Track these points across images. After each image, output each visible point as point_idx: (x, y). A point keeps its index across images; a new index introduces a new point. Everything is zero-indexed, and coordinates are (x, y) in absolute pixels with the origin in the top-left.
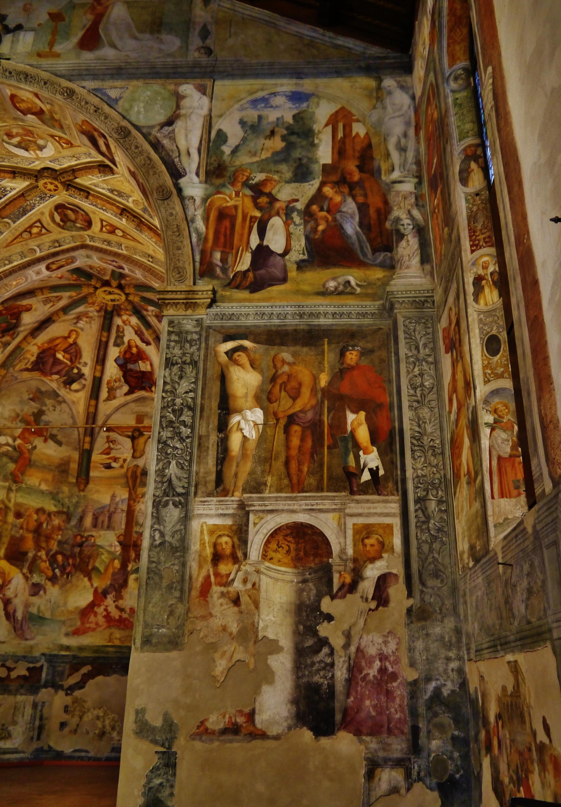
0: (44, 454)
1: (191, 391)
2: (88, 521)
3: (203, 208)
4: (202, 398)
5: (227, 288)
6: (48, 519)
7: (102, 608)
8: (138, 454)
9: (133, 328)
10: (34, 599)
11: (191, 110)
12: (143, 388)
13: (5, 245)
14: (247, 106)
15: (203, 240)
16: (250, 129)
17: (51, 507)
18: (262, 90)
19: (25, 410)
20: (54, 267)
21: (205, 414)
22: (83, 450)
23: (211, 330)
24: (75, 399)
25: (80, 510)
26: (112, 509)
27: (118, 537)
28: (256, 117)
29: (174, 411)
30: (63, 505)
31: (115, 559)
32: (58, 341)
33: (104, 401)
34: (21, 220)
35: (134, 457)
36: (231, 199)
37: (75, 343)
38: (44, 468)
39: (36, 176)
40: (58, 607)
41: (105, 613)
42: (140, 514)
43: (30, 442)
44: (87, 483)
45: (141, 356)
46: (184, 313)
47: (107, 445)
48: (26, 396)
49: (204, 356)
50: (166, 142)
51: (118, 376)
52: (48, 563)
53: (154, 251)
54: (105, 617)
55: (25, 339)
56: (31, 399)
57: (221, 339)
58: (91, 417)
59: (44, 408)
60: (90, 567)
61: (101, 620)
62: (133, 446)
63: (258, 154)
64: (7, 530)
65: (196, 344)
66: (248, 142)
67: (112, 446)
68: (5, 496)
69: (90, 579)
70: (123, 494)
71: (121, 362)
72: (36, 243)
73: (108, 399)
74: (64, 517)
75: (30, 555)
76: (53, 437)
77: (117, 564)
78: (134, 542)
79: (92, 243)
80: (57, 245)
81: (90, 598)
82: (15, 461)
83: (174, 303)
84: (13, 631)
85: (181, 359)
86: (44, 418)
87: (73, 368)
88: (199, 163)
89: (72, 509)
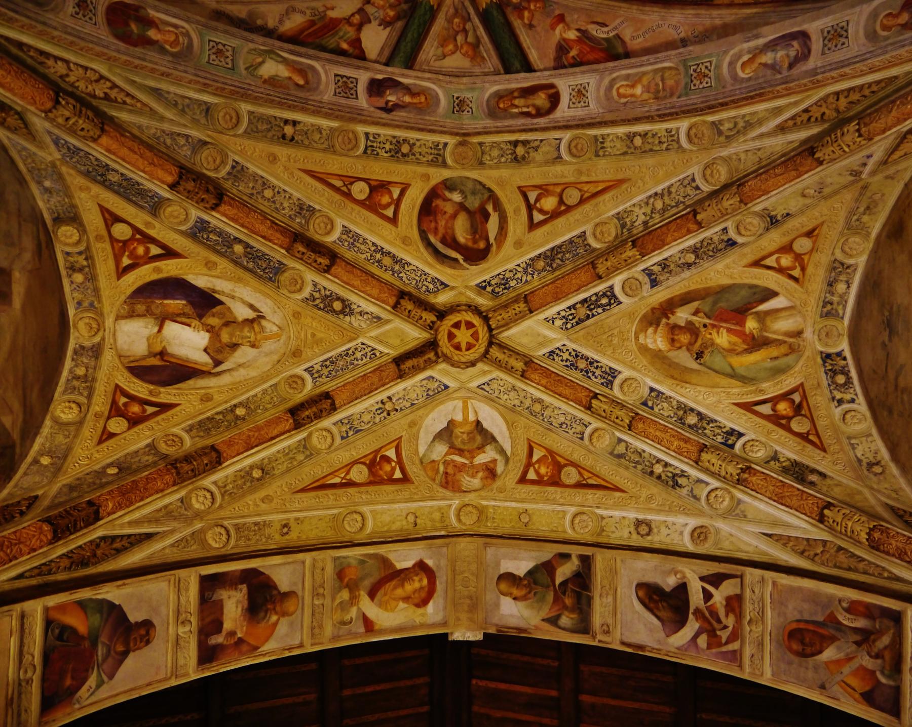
13: (624, 186)
20: (541, 99)
34: (567, 237)
53: (273, 159)
72: (558, 168)
80: (520, 151)
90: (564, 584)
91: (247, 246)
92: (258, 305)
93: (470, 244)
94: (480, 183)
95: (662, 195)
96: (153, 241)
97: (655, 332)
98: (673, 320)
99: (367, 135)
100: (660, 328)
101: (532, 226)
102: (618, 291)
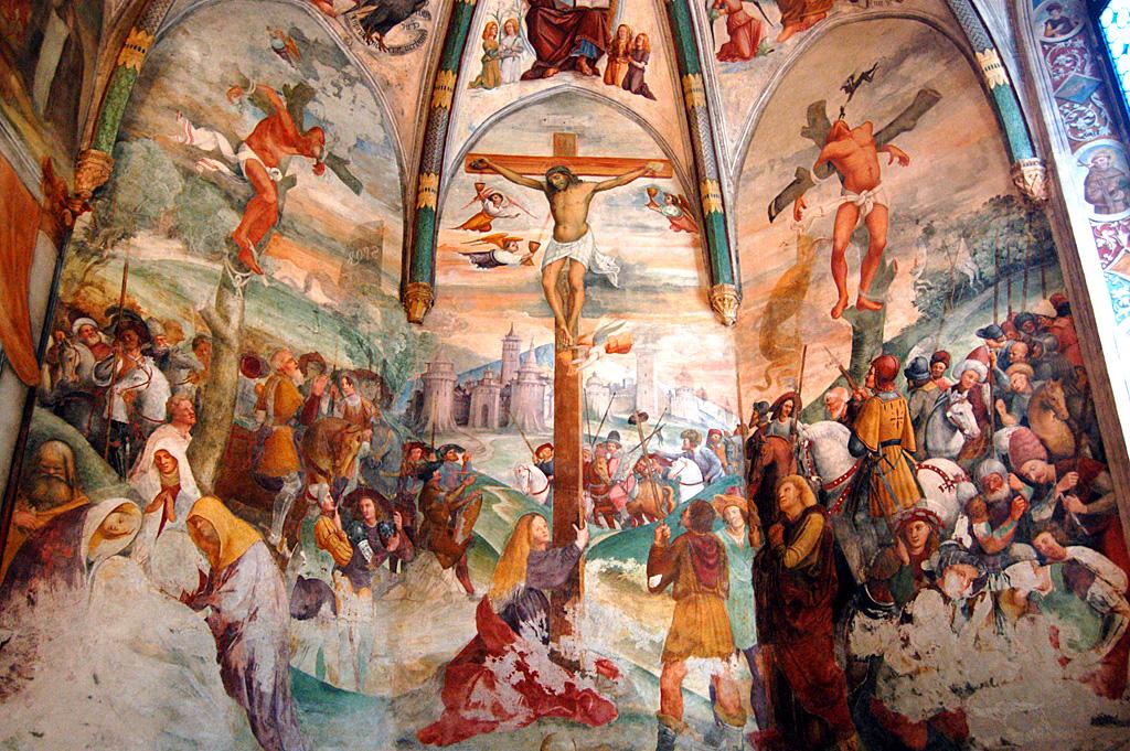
0: (318, 205)
2: (442, 406)
6: (334, 388)
7: (511, 658)
8: (569, 231)
10: (306, 629)
12: (572, 66)
17: (340, 357)
19: (265, 74)
22: (417, 211)
24: (392, 77)
25: (414, 376)
26: (510, 376)
27: (537, 454)
30: (369, 354)
31: (534, 515)
33: (472, 85)
35: (557, 236)
38: (318, 242)
40: (373, 656)
41: (520, 676)
42: (594, 389)
43: (277, 164)
44: (430, 304)
47: (478, 207)
48: (267, 43)
51: (515, 16)
52: (337, 516)
54: (519, 687)
59: (312, 83)
60: (460, 539)
61: (509, 697)
62: (553, 211)
64: (219, 405)
68: (213, 303)
69: (462, 574)
70: (538, 335)
74: (375, 389)
75: (290, 489)
76: (338, 164)
77: (542, 529)
78: (586, 465)
81: (471, 631)
82: (242, 208)
84: (249, 729)
86: (311, 106)
89: (393, 370)
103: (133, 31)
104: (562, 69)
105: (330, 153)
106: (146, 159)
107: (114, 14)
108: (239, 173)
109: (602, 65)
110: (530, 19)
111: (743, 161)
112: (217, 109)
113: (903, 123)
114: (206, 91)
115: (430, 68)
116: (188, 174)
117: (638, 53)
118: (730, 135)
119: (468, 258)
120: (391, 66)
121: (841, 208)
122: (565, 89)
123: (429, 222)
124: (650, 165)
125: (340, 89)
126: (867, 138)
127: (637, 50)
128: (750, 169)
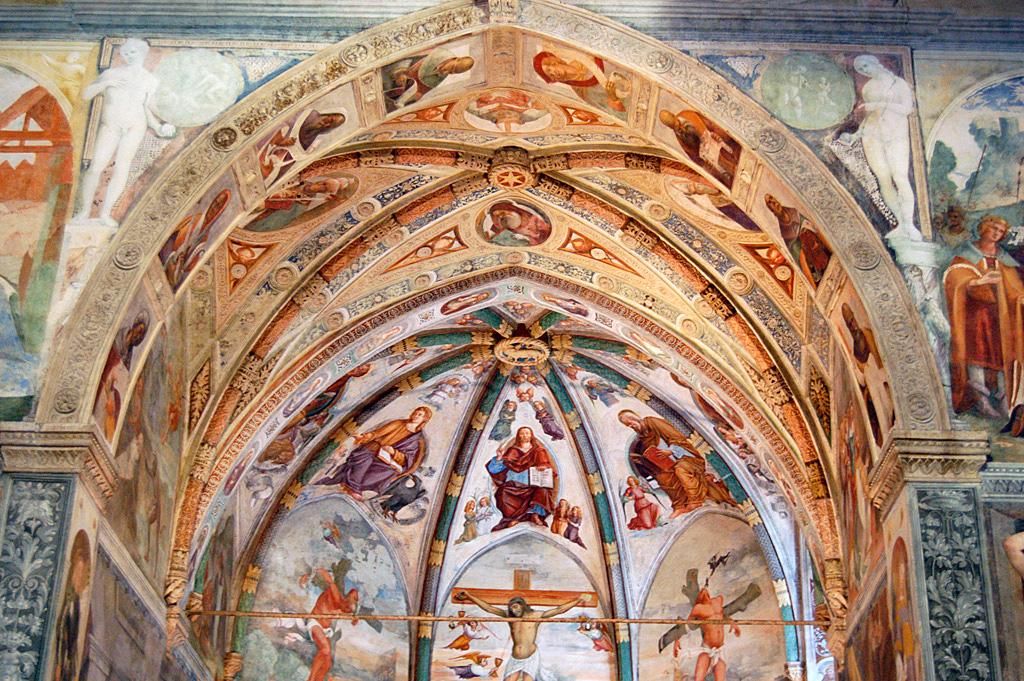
0: (355, 647)
1: (978, 618)
3: (938, 288)
4: (1000, 631)
5: (1006, 436)
8: (523, 650)
9: (535, 406)
11: (882, 104)
12: (529, 518)
14: (978, 100)
15: (948, 345)
16: (991, 142)
18: (998, 71)
19: (320, 560)
20: (455, 306)
21: (1010, 658)
22: (419, 639)
23: (992, 510)
24: (401, 539)
28: (998, 121)
29: (955, 652)
32: (391, 428)
33: (457, 542)
34: (425, 227)
35: (515, 655)
36: (983, 273)
37: (419, 431)
39: (490, 161)
45: (538, 457)
46: (940, 477)
47: (460, 631)
48: (320, 533)
49: (989, 556)
50: (849, 161)
51: (487, 495)
53: (662, 290)
55: (342, 425)
56: (327, 539)
57: (1013, 526)
58: (429, 571)
59: (350, 556)
62: (512, 634)
63: (1014, 191)
65: (971, 535)
66: (991, 168)
67: (471, 632)
71: (497, 468)
73: (463, 539)
76: (366, 613)
79: (531, 267)
80: (469, 267)
82: (310, 664)
83: (924, 460)
85: (951, 560)
86: (350, 574)
87: (408, 478)
88: (916, 204)
90: (409, 85)
91: (690, 245)
92: (690, 202)
93: (507, 212)
94: (500, 245)
95: (353, 272)
96: (763, 262)
97: (341, 186)
98: (328, 195)
99: (591, 281)
100: (337, 188)
101: (455, 230)
102: (378, 204)
103: (251, 566)
104: (521, 521)
105: (362, 607)
106: (256, 644)
107: (238, 555)
108: (308, 639)
109: (550, 520)
110: (498, 496)
111: (645, 601)
112: (294, 595)
113: (740, 604)
114: (286, 584)
115: (428, 535)
116: (280, 647)
117: (573, 517)
118: (636, 581)
119: (452, 670)
120: (400, 532)
121: (701, 655)
122: (524, 532)
123: (427, 648)
124: (582, 597)
125: (367, 554)
126: (719, 609)
127: (573, 516)
128: (651, 608)
